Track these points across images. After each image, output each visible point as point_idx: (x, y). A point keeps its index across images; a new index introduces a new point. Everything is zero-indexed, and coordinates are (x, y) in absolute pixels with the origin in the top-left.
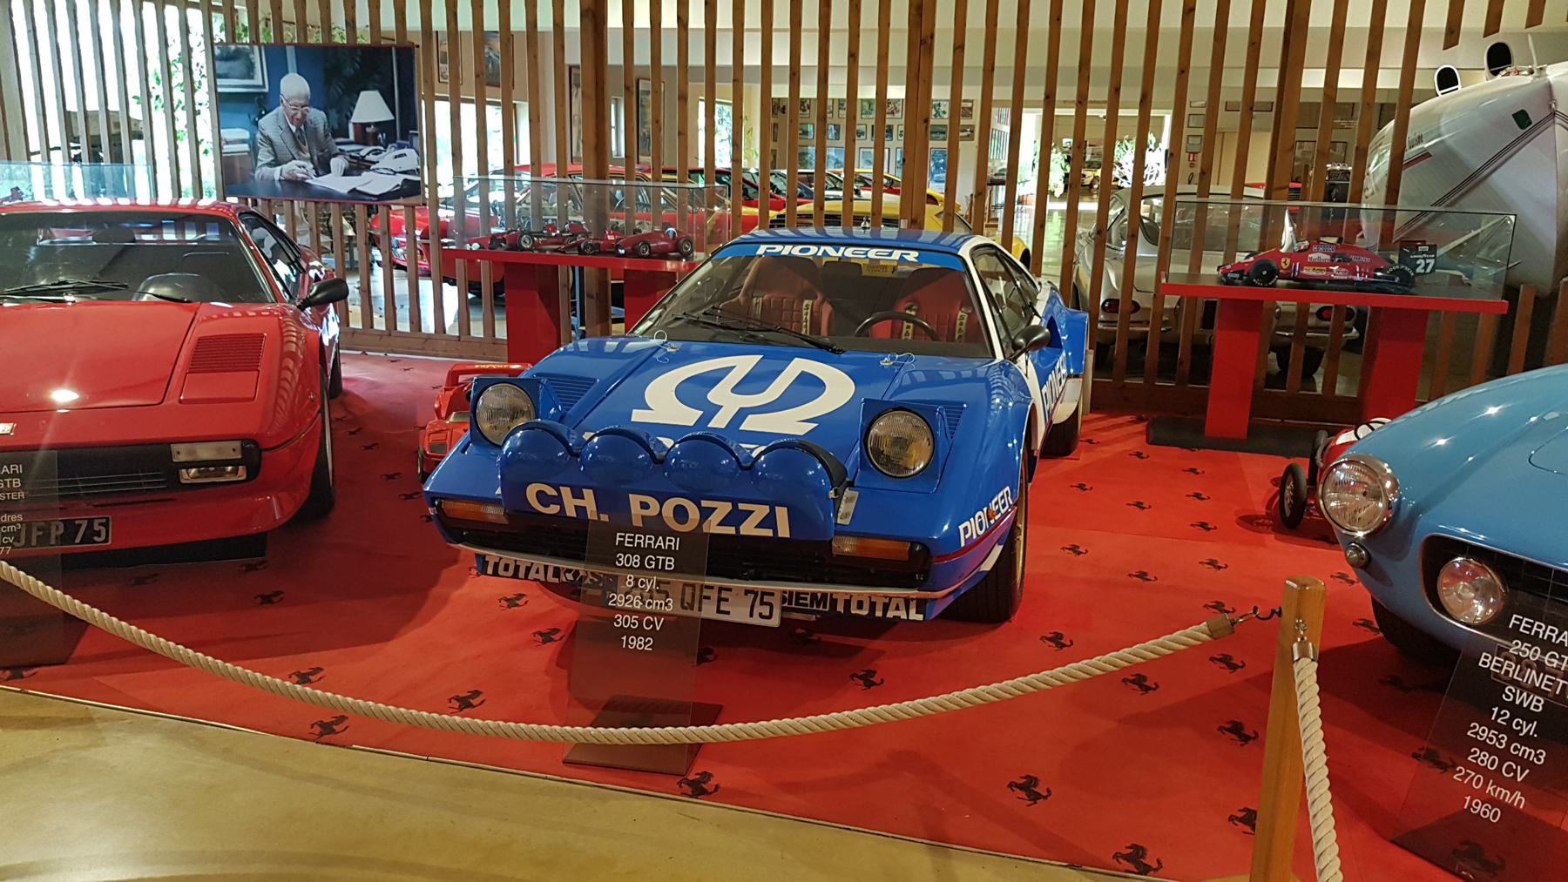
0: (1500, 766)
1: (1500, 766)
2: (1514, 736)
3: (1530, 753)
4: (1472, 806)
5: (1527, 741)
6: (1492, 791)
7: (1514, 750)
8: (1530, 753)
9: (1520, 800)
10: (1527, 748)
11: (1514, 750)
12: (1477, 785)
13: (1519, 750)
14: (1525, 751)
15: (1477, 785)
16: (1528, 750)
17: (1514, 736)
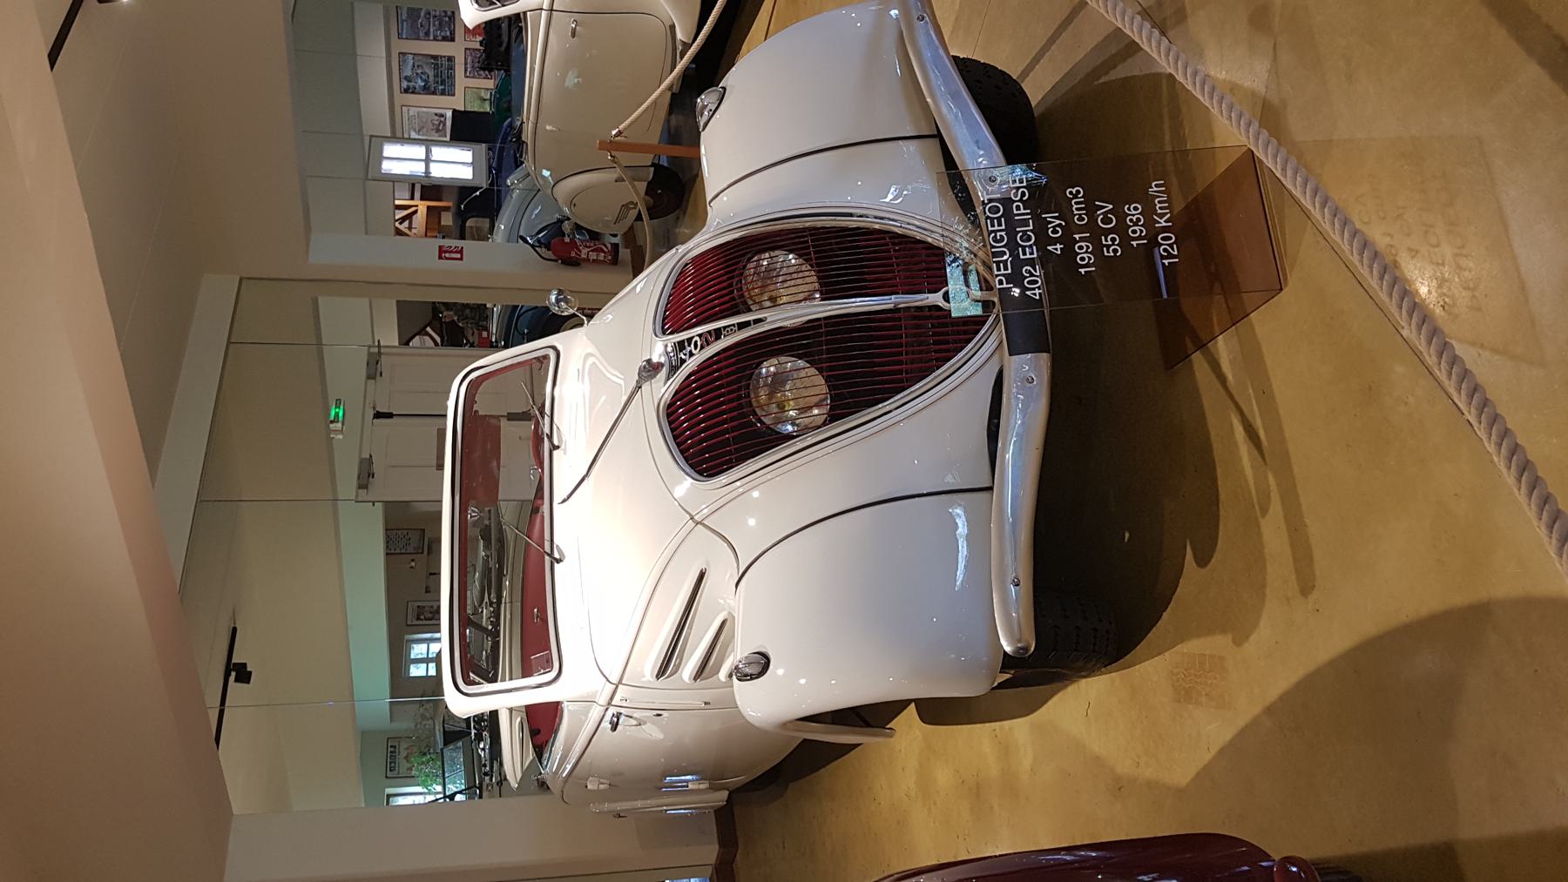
0: (1111, 231)
1: (1111, 231)
2: (1069, 230)
3: (1076, 203)
4: (1140, 235)
5: (1065, 214)
6: (1165, 218)
7: (1084, 219)
8: (1076, 203)
9: (1156, 186)
10: (1074, 209)
11: (1084, 219)
12: (1171, 238)
13: (1080, 215)
14: (1077, 209)
15: (1171, 238)
16: (1075, 206)
17: (1069, 230)
